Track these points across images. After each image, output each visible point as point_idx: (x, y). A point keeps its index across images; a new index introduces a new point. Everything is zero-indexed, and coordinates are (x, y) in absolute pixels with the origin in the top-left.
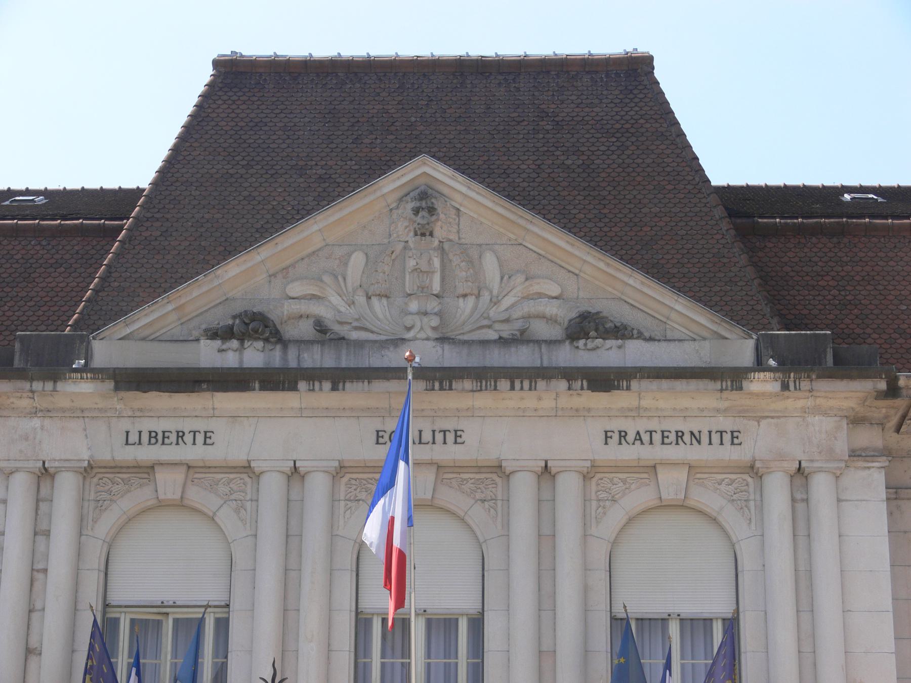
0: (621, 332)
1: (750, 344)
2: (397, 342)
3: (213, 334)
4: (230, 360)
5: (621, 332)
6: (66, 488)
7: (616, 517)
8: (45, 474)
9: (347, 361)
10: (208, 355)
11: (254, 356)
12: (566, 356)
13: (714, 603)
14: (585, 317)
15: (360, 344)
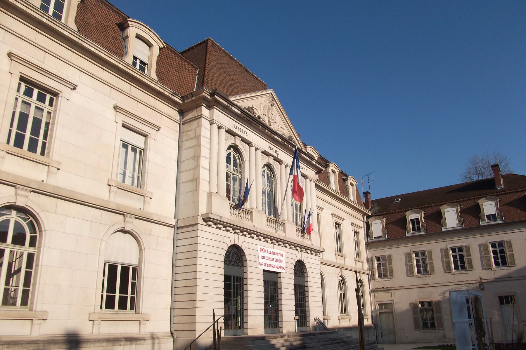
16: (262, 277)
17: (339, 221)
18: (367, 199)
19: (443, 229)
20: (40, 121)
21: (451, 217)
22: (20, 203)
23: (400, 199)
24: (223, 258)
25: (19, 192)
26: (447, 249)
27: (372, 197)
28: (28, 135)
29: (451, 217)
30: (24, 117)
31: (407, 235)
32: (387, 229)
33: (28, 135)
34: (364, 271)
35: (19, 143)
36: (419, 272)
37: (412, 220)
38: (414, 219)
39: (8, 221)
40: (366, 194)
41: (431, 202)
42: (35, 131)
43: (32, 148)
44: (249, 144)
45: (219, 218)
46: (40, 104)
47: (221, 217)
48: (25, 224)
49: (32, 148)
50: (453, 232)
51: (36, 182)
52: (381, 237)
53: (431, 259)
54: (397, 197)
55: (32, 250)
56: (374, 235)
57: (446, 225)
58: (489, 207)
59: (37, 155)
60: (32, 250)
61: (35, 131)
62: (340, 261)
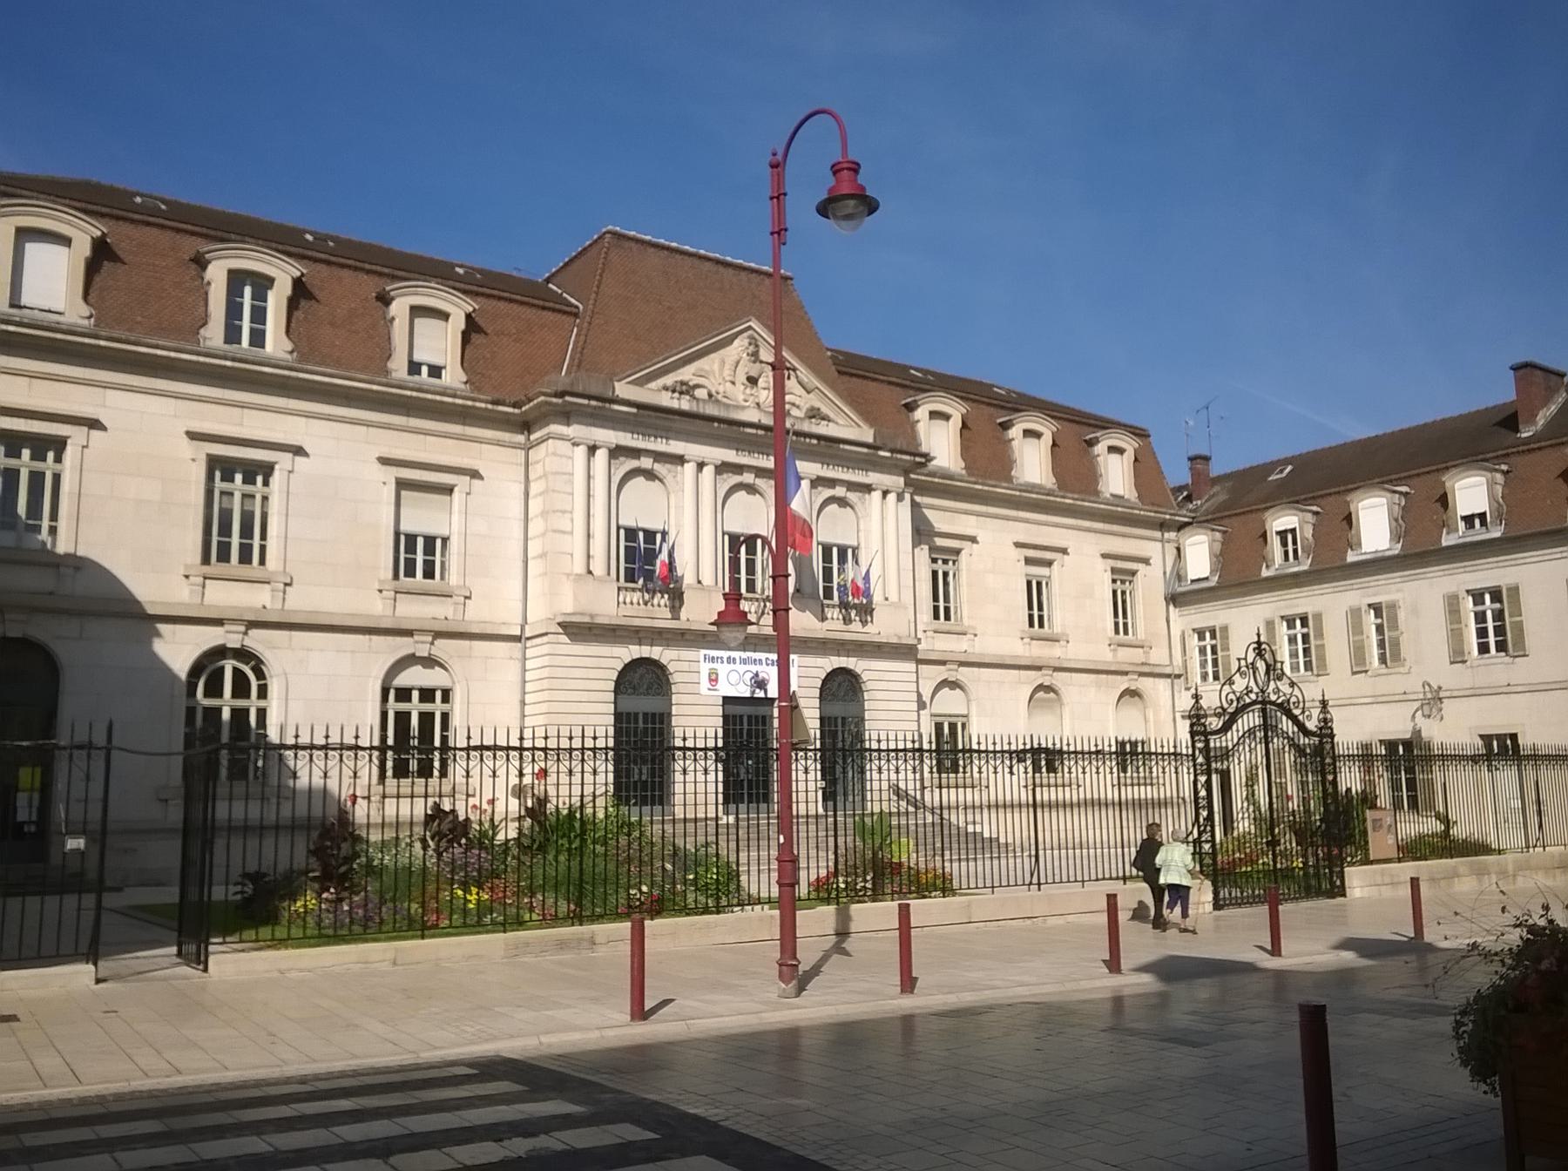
0: (825, 418)
1: (872, 432)
2: (744, 408)
3: (666, 388)
4: (675, 404)
5: (825, 418)
6: (601, 455)
7: (820, 500)
8: (592, 449)
9: (722, 413)
10: (667, 400)
11: (685, 404)
12: (807, 427)
13: (855, 544)
14: (812, 409)
15: (727, 406)
16: (720, 711)
17: (1048, 555)
18: (1195, 473)
19: (1351, 557)
20: (252, 514)
21: (1375, 521)
22: (234, 642)
23: (1289, 468)
24: (612, 686)
25: (227, 627)
26: (1359, 609)
27: (1216, 469)
28: (235, 540)
29: (1375, 521)
30: (226, 516)
31: (1265, 573)
32: (1223, 559)
33: (235, 540)
34: (1146, 669)
35: (224, 556)
36: (1383, 659)
37: (1282, 534)
38: (1286, 531)
39: (222, 668)
40: (1199, 460)
41: (1326, 479)
42: (247, 531)
43: (245, 557)
44: (680, 460)
45: (587, 619)
46: (249, 488)
47: (592, 616)
48: (247, 670)
49: (245, 557)
50: (1378, 565)
51: (250, 609)
52: (1206, 579)
53: (1320, 634)
54: (1286, 462)
55: (262, 703)
56: (1192, 575)
57: (1360, 545)
58: (1471, 492)
59: (254, 569)
60: (262, 703)
61: (247, 531)
62: (1039, 651)
